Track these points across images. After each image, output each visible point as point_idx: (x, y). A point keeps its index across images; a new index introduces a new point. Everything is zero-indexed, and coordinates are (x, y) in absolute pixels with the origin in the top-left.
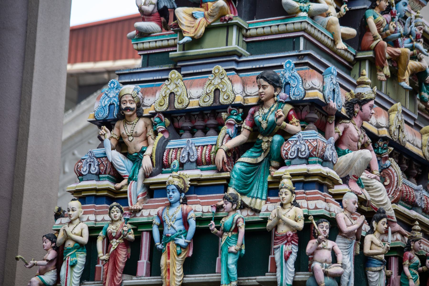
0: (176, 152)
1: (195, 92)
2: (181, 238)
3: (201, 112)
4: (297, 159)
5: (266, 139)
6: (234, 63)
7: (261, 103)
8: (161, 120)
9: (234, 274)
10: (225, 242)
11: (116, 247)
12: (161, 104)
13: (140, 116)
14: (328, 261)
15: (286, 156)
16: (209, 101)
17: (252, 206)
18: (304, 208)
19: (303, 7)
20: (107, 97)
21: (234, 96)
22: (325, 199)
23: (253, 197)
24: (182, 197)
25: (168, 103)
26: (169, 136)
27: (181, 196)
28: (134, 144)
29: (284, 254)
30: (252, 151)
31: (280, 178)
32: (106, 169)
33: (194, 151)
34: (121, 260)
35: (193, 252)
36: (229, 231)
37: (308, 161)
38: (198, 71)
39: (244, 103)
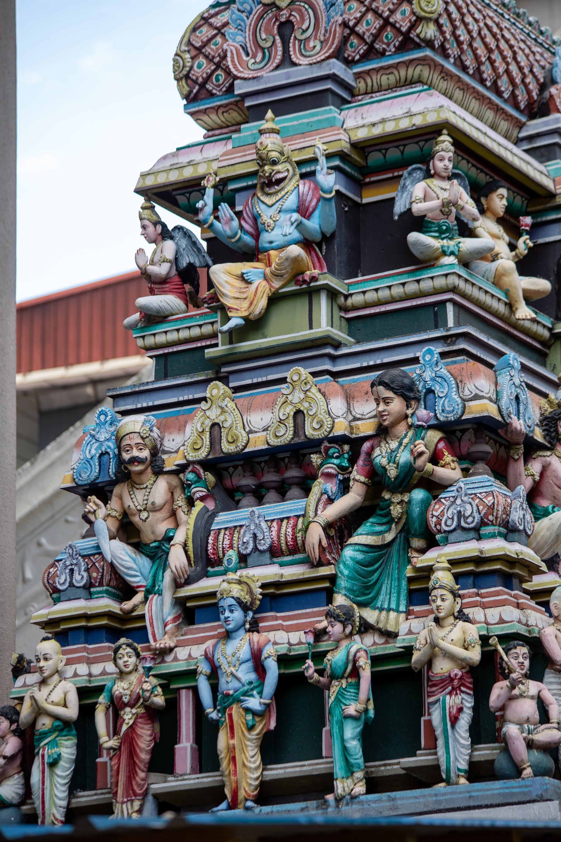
0: (232, 535)
1: (259, 419)
2: (252, 696)
3: (273, 456)
4: (459, 531)
5: (397, 498)
6: (326, 360)
7: (383, 432)
8: (199, 476)
9: (357, 757)
10: (337, 698)
11: (131, 722)
12: (197, 447)
13: (159, 472)
14: (531, 719)
15: (438, 527)
16: (286, 435)
17: (381, 625)
18: (480, 622)
19: (448, 247)
20: (94, 441)
21: (331, 422)
22: (518, 603)
23: (381, 609)
24: (249, 619)
25: (208, 443)
26: (216, 506)
27: (246, 616)
28: (152, 526)
30: (373, 523)
31: (429, 570)
32: (102, 576)
33: (265, 530)
34: (142, 745)
35: (278, 721)
36: (342, 677)
37: (479, 534)
38: (260, 380)
39: (352, 433)
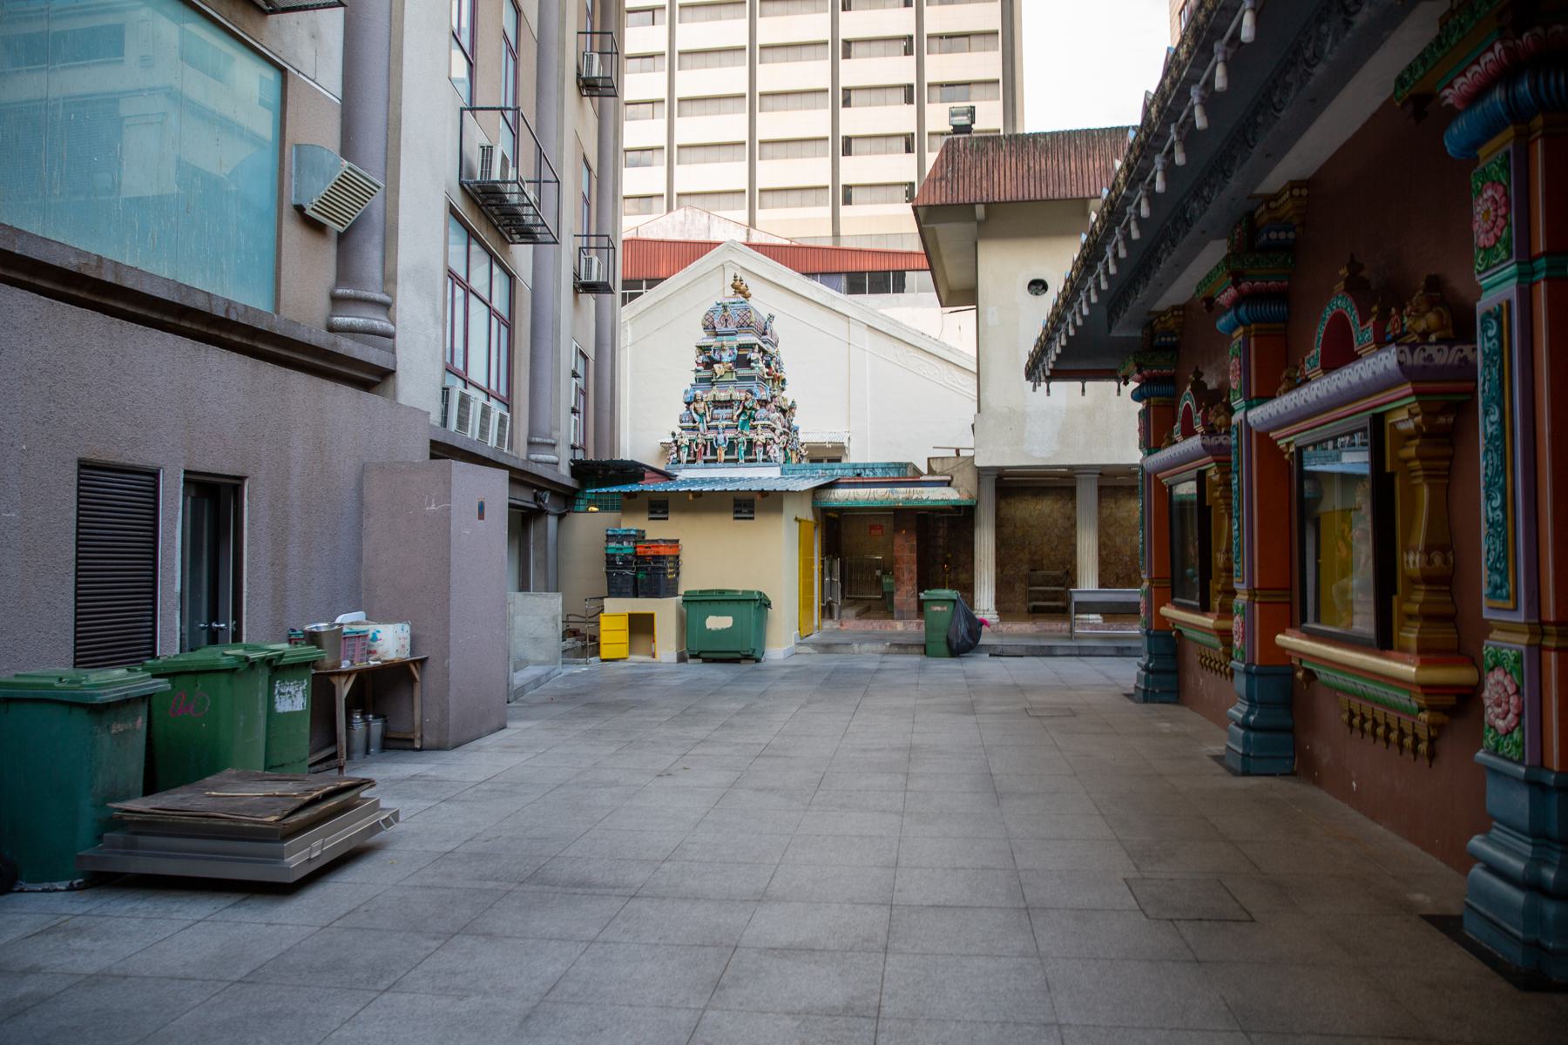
29: (759, 450)
